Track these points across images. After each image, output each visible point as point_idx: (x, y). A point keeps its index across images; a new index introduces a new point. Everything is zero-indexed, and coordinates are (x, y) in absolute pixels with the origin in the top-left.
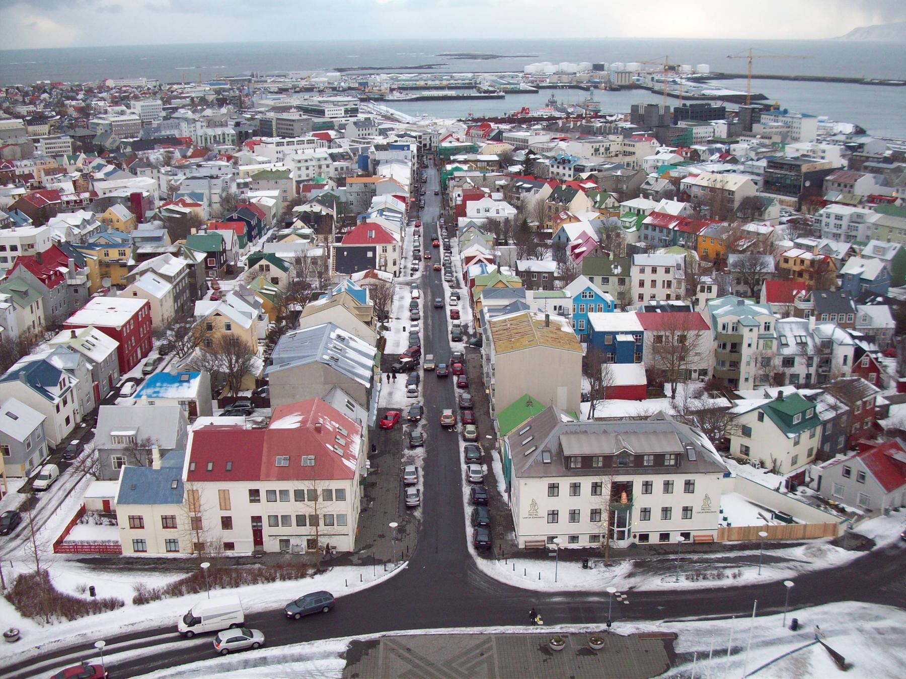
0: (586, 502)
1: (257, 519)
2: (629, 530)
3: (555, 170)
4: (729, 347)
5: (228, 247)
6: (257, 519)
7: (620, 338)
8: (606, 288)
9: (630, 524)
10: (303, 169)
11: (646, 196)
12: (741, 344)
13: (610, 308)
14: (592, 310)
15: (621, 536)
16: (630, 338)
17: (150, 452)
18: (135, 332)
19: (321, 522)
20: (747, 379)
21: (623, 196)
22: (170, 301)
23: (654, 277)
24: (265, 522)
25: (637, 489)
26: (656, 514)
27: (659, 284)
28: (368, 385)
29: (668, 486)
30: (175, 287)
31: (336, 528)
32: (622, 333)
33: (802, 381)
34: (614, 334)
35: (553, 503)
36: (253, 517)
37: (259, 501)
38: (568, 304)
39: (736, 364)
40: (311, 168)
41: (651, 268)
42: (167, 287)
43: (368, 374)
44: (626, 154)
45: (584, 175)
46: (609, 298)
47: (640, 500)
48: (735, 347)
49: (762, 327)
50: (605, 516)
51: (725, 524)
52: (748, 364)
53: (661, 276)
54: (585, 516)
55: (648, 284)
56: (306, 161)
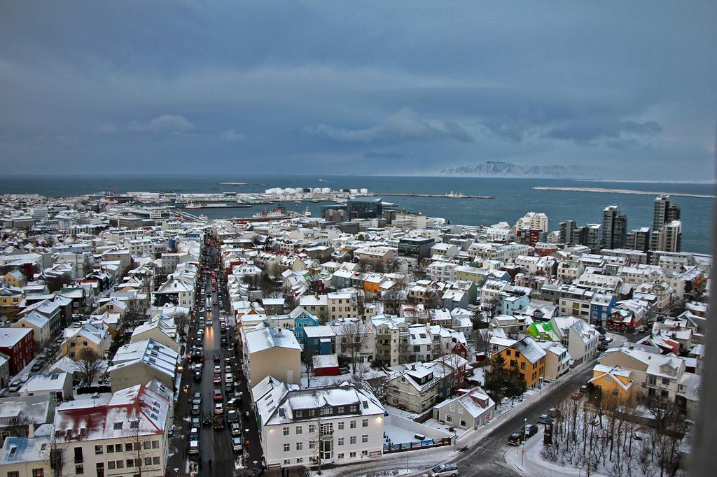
0: (306, 437)
1: (100, 465)
2: (332, 452)
3: (283, 247)
4: (384, 342)
5: (87, 295)
6: (100, 465)
7: (322, 341)
8: (313, 312)
9: (332, 449)
10: (136, 249)
11: (335, 261)
12: (390, 340)
13: (315, 324)
14: (306, 325)
15: (328, 457)
16: (329, 340)
17: (27, 426)
18: (22, 350)
19: (143, 463)
20: (395, 360)
21: (322, 261)
22: (48, 329)
23: (340, 305)
24: (106, 466)
25: (335, 427)
26: (347, 441)
27: (344, 309)
28: (173, 375)
29: (353, 426)
30: (51, 320)
31: (153, 466)
32: (324, 338)
33: (425, 359)
34: (319, 338)
35: (286, 439)
36: (97, 464)
37: (102, 453)
38: (292, 322)
39: (388, 352)
40: (140, 248)
41: (338, 301)
42: (47, 320)
43: (173, 368)
44: (323, 237)
45: (300, 250)
46: (315, 318)
47: (337, 434)
48: (387, 342)
49: (401, 330)
50: (318, 445)
51: (387, 444)
52: (395, 351)
53: (344, 304)
54: (306, 446)
55: (337, 309)
56: (137, 243)
